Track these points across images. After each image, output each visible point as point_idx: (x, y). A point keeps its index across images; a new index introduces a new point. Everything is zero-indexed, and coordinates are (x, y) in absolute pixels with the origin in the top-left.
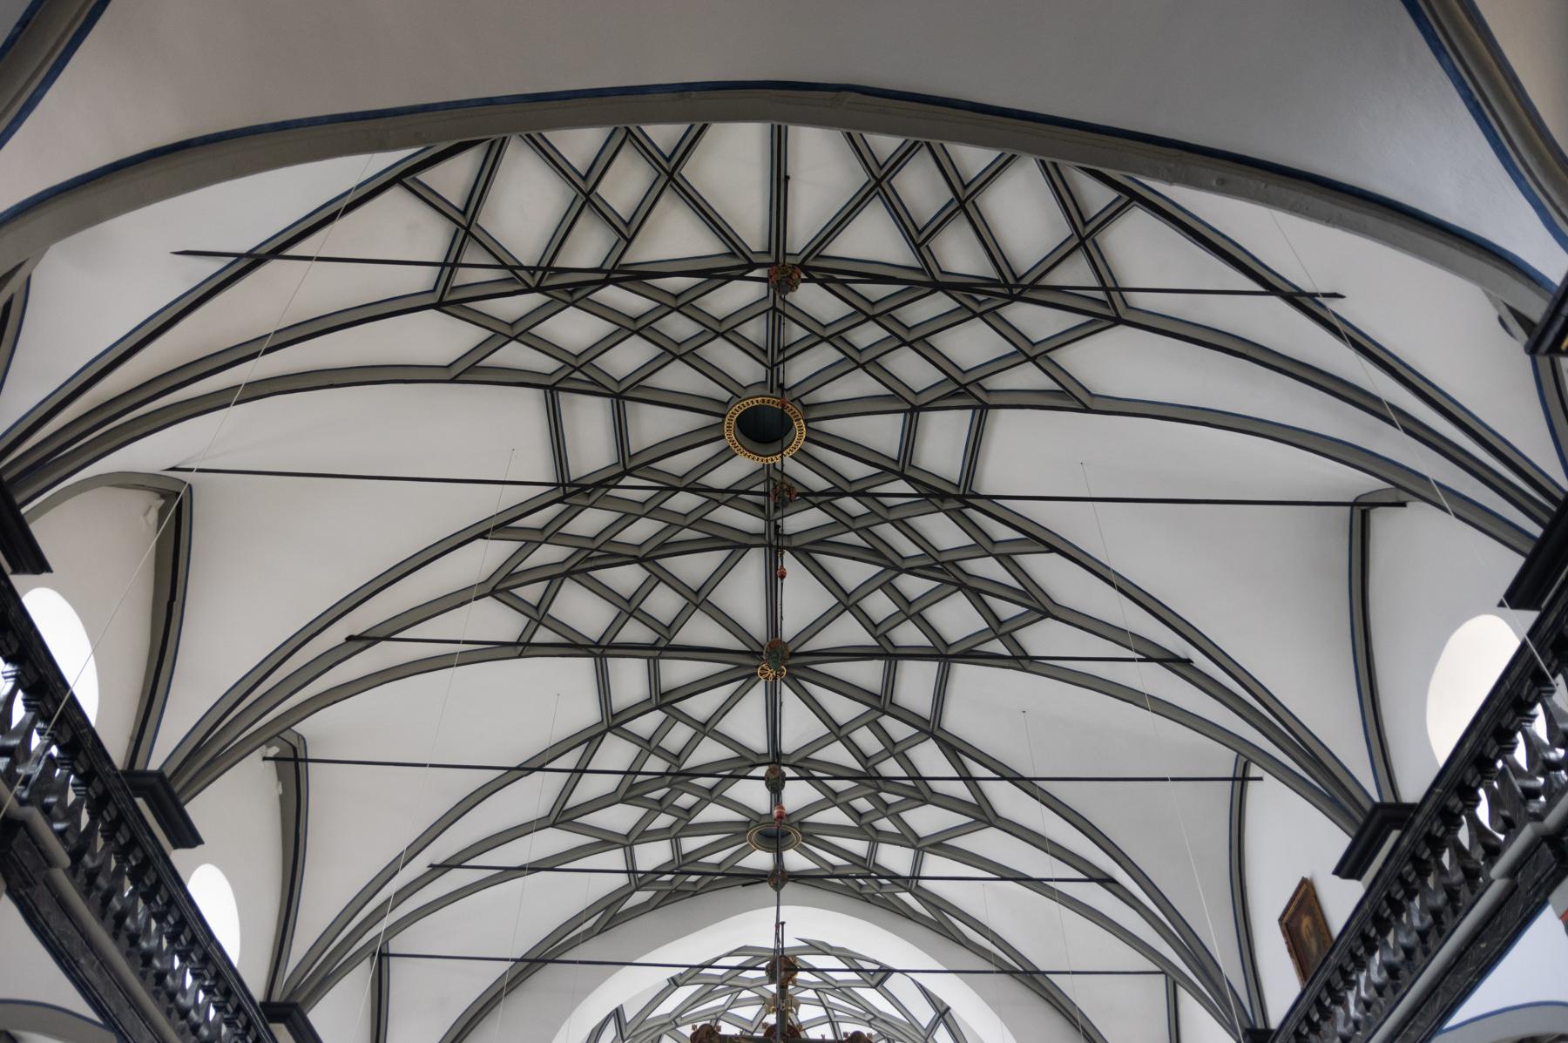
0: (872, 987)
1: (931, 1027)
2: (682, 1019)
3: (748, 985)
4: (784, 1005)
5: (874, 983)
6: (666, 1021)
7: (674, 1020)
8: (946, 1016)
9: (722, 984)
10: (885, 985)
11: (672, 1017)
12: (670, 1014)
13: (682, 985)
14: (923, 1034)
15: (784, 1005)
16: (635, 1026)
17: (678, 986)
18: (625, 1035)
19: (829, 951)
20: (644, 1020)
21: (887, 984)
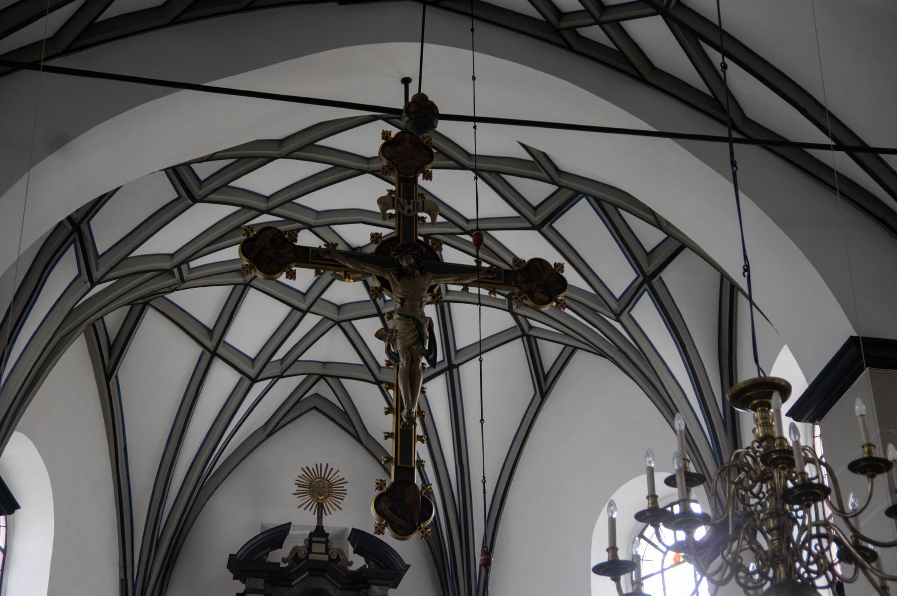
0: (534, 227)
1: (627, 298)
2: (190, 270)
3: (311, 220)
4: (411, 207)
5: (537, 220)
6: (167, 265)
7: (178, 266)
8: (655, 281)
9: (268, 212)
10: (556, 225)
11: (177, 260)
12: (172, 255)
13: (203, 200)
14: (614, 305)
15: (411, 207)
16: (112, 262)
17: (195, 201)
18: (97, 275)
19: (465, 161)
20: (126, 257)
21: (558, 225)
